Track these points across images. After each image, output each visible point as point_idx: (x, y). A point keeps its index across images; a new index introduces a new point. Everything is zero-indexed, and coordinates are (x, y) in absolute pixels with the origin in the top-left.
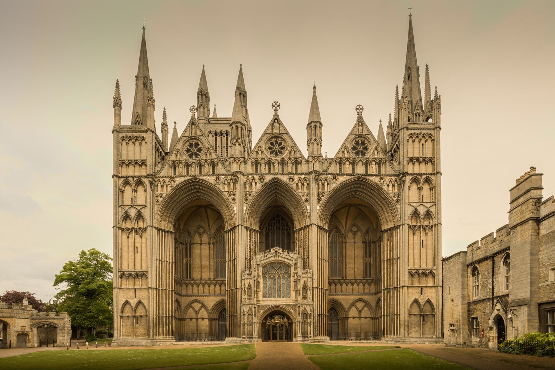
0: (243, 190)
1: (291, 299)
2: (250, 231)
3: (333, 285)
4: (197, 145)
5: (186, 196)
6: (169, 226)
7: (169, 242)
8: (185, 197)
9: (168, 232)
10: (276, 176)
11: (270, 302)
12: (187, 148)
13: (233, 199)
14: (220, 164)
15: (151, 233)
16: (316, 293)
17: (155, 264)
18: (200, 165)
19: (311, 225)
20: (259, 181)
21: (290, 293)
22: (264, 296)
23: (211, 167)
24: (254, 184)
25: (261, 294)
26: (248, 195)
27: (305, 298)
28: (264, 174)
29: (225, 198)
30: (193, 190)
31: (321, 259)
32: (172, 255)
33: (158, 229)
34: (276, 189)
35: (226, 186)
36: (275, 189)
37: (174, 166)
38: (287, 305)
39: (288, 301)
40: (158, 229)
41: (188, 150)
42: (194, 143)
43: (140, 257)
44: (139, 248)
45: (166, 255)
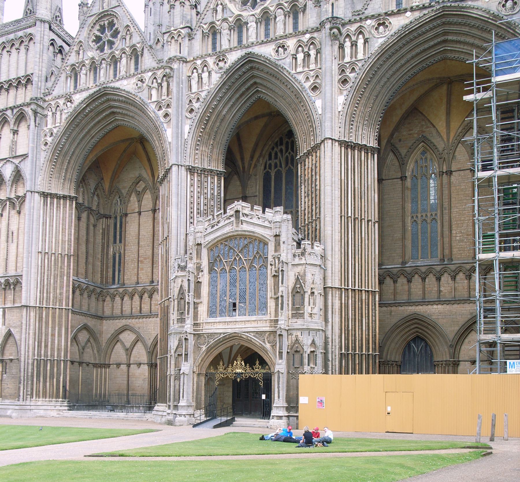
0: (185, 92)
1: (268, 317)
2: (200, 175)
3: (388, 281)
4: (111, 24)
5: (95, 125)
6: (67, 185)
7: (65, 216)
8: (92, 128)
9: (65, 197)
10: (250, 50)
11: (221, 326)
12: (96, 36)
13: (166, 115)
14: (146, 51)
15: (34, 202)
16: (335, 301)
17: (35, 260)
18: (115, 61)
19: (323, 141)
20: (216, 68)
21: (266, 304)
22: (211, 313)
23: (133, 61)
24: (205, 75)
25: (203, 309)
26: (194, 101)
27: (297, 312)
28: (226, 51)
29: (152, 115)
30: (104, 111)
31: (350, 221)
32: (70, 240)
33: (44, 195)
34: (255, 83)
35: (154, 92)
36: (250, 79)
37: (75, 73)
38: (257, 332)
39: (260, 324)
40: (44, 195)
41: (98, 39)
42: (106, 22)
43: (15, 251)
44: (15, 234)
45: (57, 242)
